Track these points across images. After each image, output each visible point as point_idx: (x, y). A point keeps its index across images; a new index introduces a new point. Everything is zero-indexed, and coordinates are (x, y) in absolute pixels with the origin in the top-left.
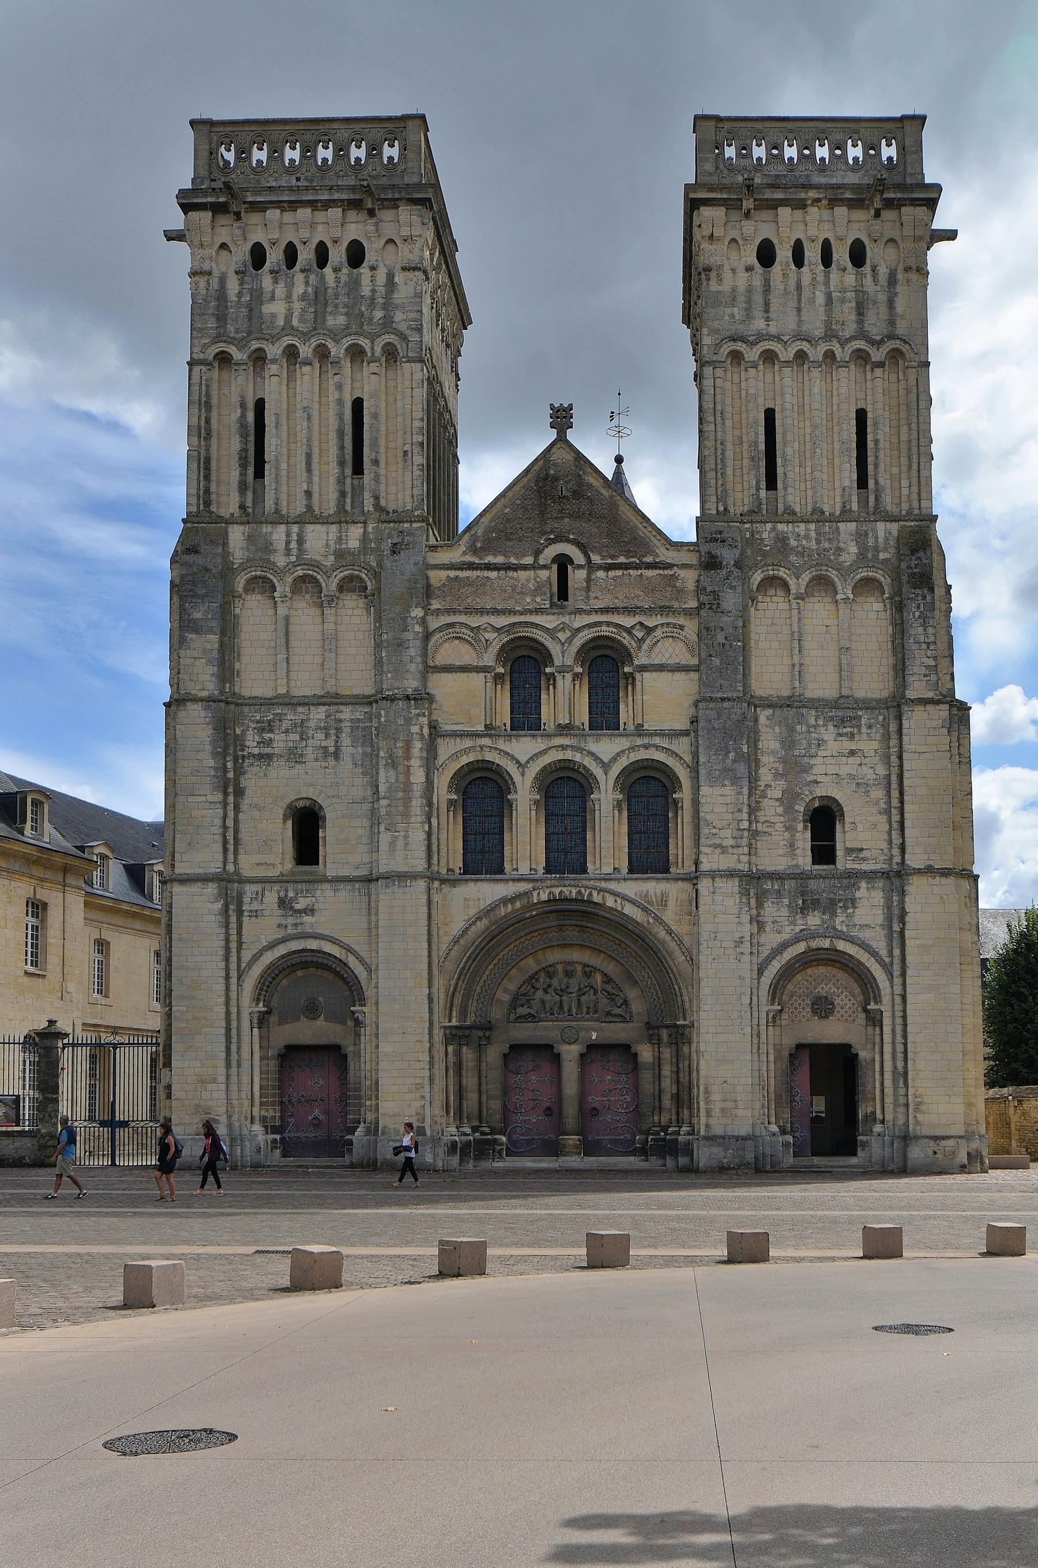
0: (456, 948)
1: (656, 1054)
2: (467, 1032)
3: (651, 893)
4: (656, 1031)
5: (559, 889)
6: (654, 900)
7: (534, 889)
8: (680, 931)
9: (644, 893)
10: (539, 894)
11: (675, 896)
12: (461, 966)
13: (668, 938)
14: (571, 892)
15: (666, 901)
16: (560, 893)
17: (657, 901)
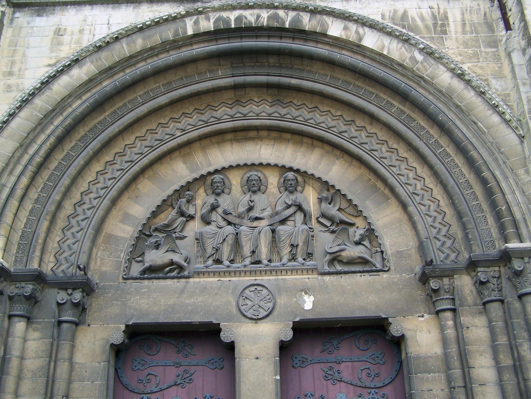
0: (24, 113)
1: (451, 332)
2: (29, 288)
3: (413, 13)
4: (446, 281)
5: (237, 13)
6: (419, 23)
7: (188, 14)
8: (479, 71)
9: (400, 13)
10: (196, 23)
11: (459, 18)
12: (31, 151)
13: (458, 85)
14: (258, 17)
15: (443, 25)
16: (238, 19)
17: (427, 27)
